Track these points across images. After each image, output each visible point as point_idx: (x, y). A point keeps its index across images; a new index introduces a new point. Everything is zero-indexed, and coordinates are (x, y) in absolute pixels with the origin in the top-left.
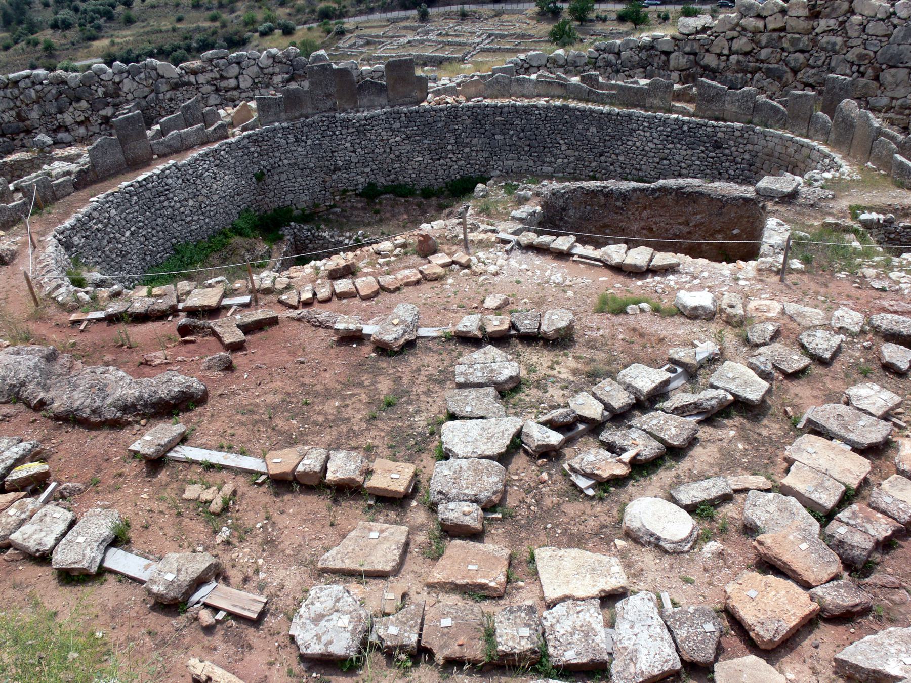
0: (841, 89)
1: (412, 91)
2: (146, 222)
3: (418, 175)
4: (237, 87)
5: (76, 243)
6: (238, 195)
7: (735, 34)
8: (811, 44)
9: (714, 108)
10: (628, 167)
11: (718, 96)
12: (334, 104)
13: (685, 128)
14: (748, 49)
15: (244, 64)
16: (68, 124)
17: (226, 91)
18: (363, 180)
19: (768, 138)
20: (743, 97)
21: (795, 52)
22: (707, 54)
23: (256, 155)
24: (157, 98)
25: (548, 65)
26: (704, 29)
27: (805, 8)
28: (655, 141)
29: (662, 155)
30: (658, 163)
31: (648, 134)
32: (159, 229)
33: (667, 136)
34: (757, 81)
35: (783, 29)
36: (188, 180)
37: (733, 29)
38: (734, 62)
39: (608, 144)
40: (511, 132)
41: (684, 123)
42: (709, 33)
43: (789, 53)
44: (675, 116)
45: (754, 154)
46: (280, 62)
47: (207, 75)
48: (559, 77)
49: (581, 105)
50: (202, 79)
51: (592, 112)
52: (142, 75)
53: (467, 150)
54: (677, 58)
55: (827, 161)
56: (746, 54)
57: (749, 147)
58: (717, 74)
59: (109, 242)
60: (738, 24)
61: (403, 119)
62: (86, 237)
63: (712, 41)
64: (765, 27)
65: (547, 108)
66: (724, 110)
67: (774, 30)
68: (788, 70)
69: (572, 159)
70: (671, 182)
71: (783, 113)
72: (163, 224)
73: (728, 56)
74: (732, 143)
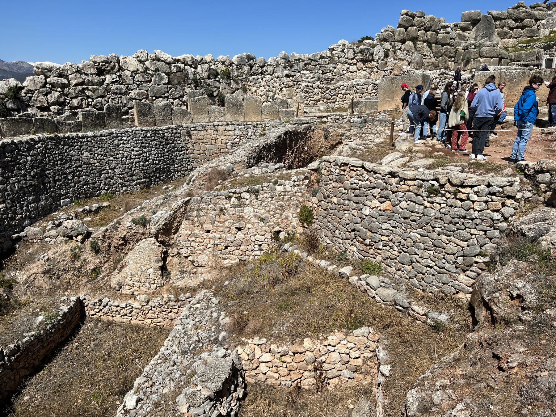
14: (62, 100)
21: (97, 98)
27: (94, 68)
30: (143, 166)
31: (129, 145)
60: (46, 83)
67: (76, 85)
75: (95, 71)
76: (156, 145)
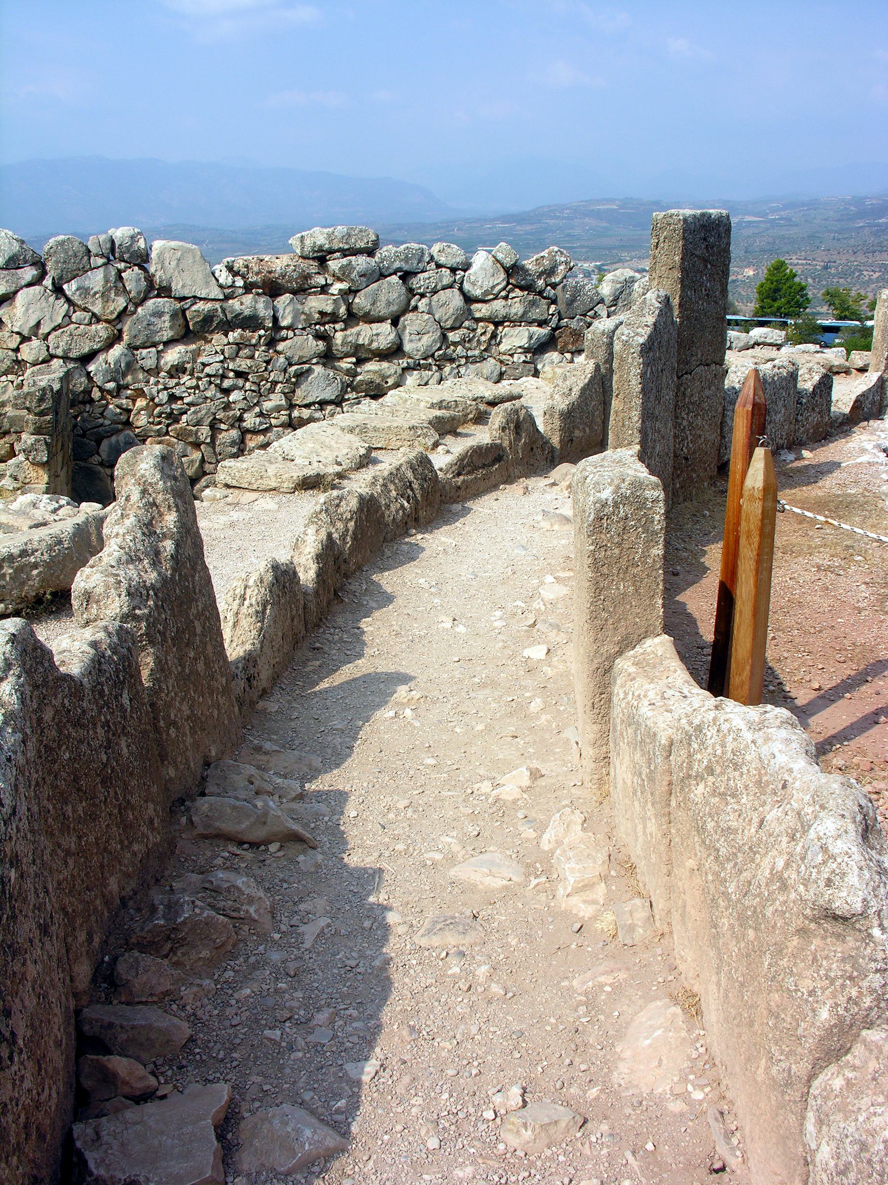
4: (395, 351)
46: (528, 287)
52: (96, 280)
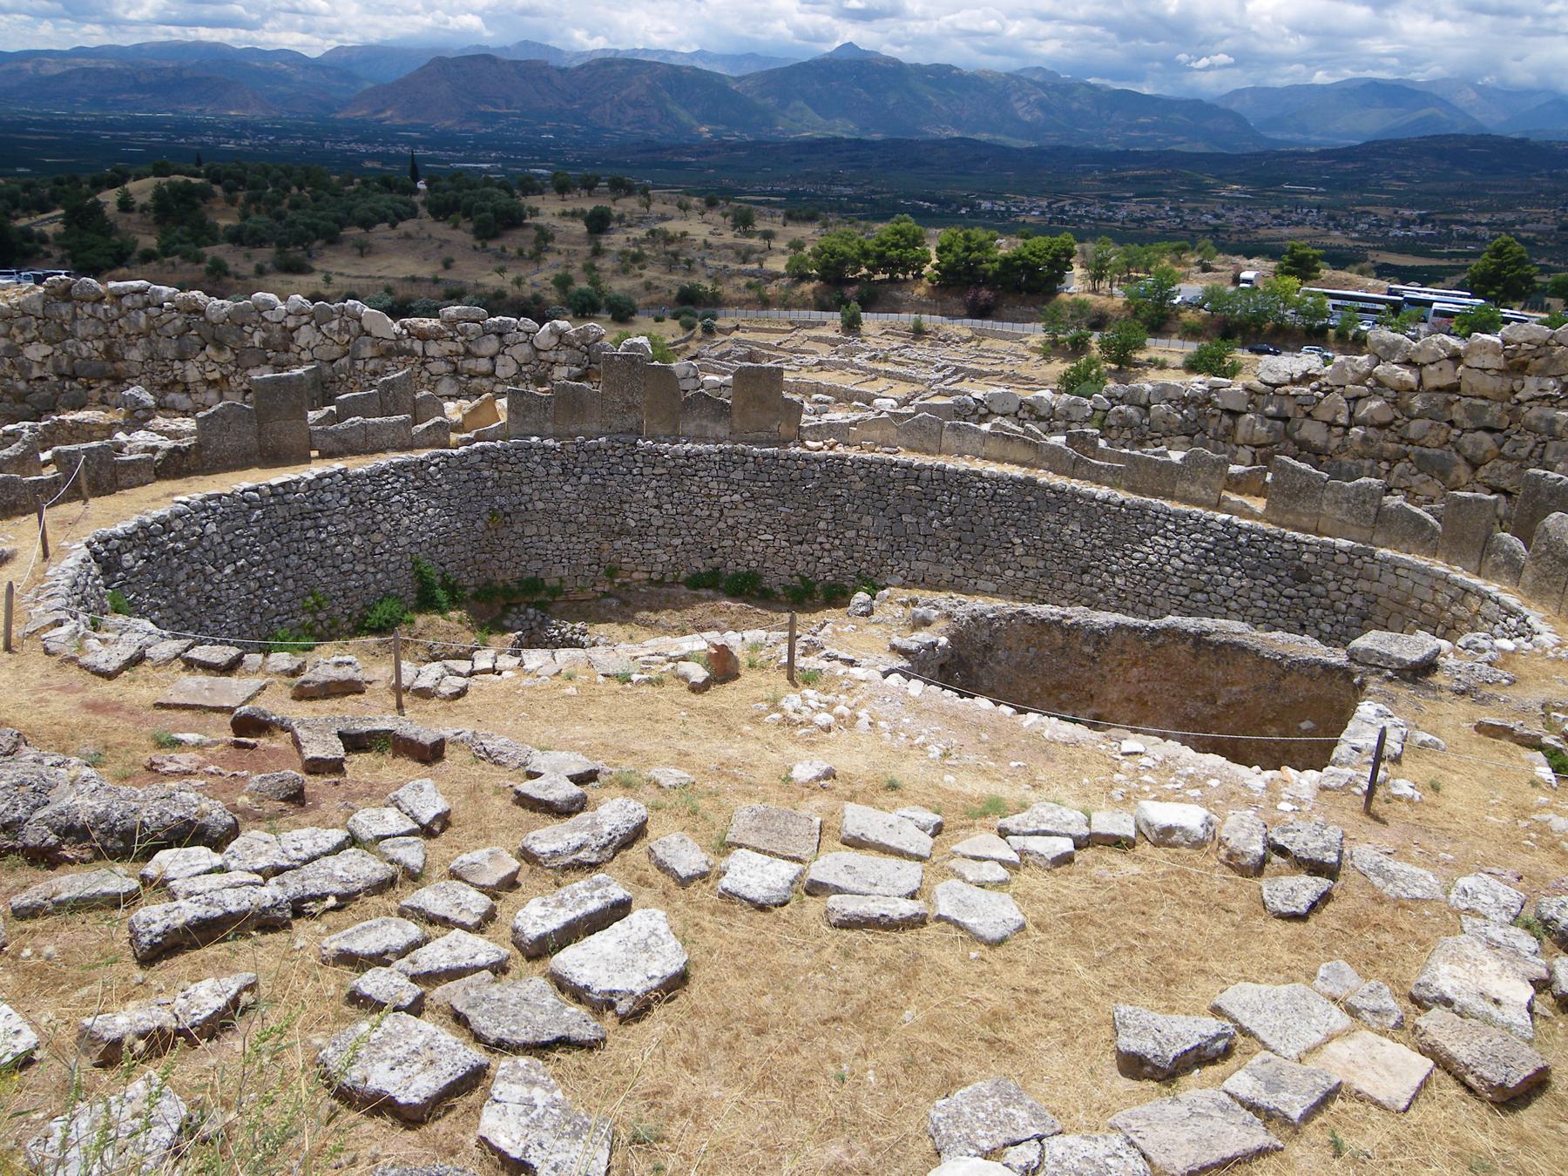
0: (1551, 496)
1: (773, 421)
2: (269, 557)
3: (761, 564)
5: (126, 565)
6: (445, 544)
7: (1364, 390)
8: (1507, 418)
9: (1300, 509)
10: (1131, 597)
11: (1310, 489)
12: (640, 423)
13: (1242, 539)
14: (1387, 418)
15: (509, 338)
16: (190, 379)
17: (471, 377)
18: (666, 558)
19: (1399, 572)
20: (1358, 495)
21: (1477, 430)
22: (1307, 421)
23: (490, 484)
24: (353, 364)
25: (1021, 414)
26: (1307, 378)
27: (1497, 354)
28: (1184, 556)
29: (1196, 584)
30: (1186, 597)
31: (1172, 544)
32: (289, 573)
33: (1208, 550)
34: (1400, 476)
35: (1454, 388)
36: (362, 503)
37: (1360, 382)
38: (1357, 439)
39: (1098, 552)
40: (931, 514)
41: (1240, 530)
42: (1314, 385)
43: (1463, 430)
44: (1227, 517)
45: (1371, 598)
47: (444, 344)
48: (1029, 432)
49: (1059, 481)
50: (433, 349)
51: (1075, 494)
52: (335, 325)
53: (851, 534)
54: (1252, 424)
55: (1513, 621)
56: (1381, 426)
57: (1363, 585)
58: (1324, 458)
59: (189, 577)
60: (1369, 374)
61: (750, 466)
62: (148, 559)
63: (1319, 399)
64: (1420, 382)
65: (998, 480)
66: (1318, 514)
67: (1438, 389)
68: (1461, 461)
69: (1031, 573)
70: (1189, 623)
71: (1434, 529)
72: (300, 567)
73: (1347, 428)
74: (1329, 574)
75: (1498, 362)
76: (1255, 569)
